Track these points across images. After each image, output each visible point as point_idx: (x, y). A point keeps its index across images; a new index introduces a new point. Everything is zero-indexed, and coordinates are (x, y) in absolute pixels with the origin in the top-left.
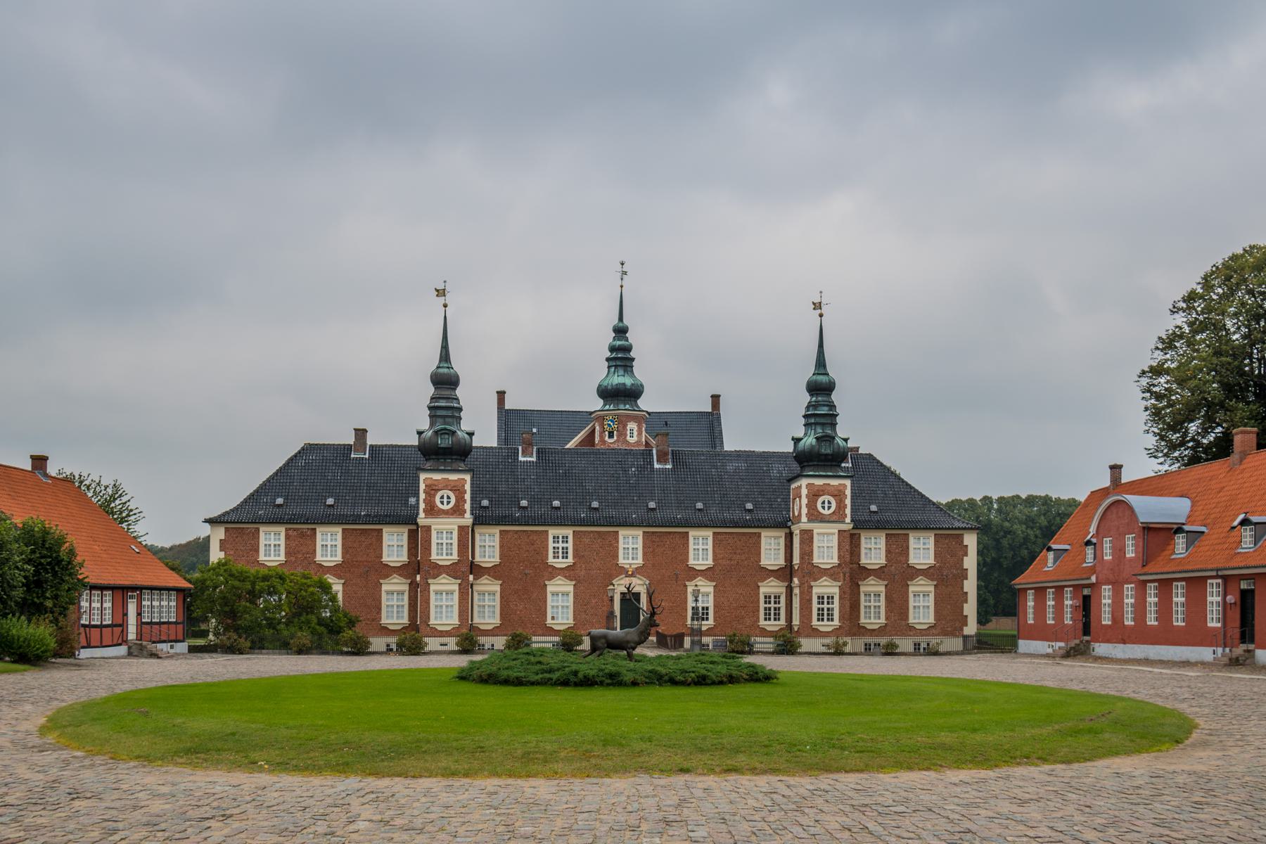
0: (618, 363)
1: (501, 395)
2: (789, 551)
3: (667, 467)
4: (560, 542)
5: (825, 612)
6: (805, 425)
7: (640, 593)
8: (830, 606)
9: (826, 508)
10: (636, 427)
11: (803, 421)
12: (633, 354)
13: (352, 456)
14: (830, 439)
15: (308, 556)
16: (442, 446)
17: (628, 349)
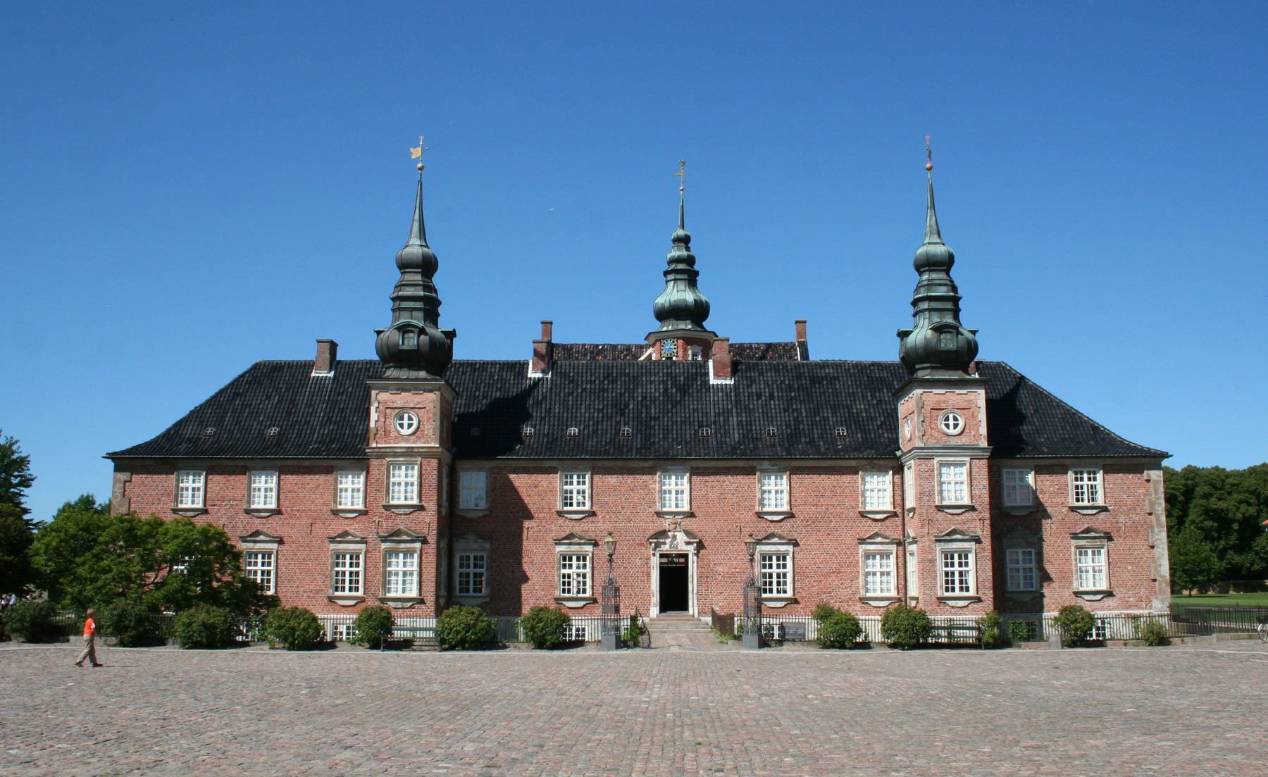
0: (679, 276)
1: (547, 325)
2: (898, 492)
3: (728, 382)
4: (575, 483)
5: (957, 578)
6: (915, 315)
7: (687, 555)
8: (963, 569)
9: (951, 426)
10: (700, 351)
11: (912, 310)
12: (696, 267)
13: (313, 375)
14: (954, 329)
15: (235, 502)
16: (404, 348)
17: (690, 260)
